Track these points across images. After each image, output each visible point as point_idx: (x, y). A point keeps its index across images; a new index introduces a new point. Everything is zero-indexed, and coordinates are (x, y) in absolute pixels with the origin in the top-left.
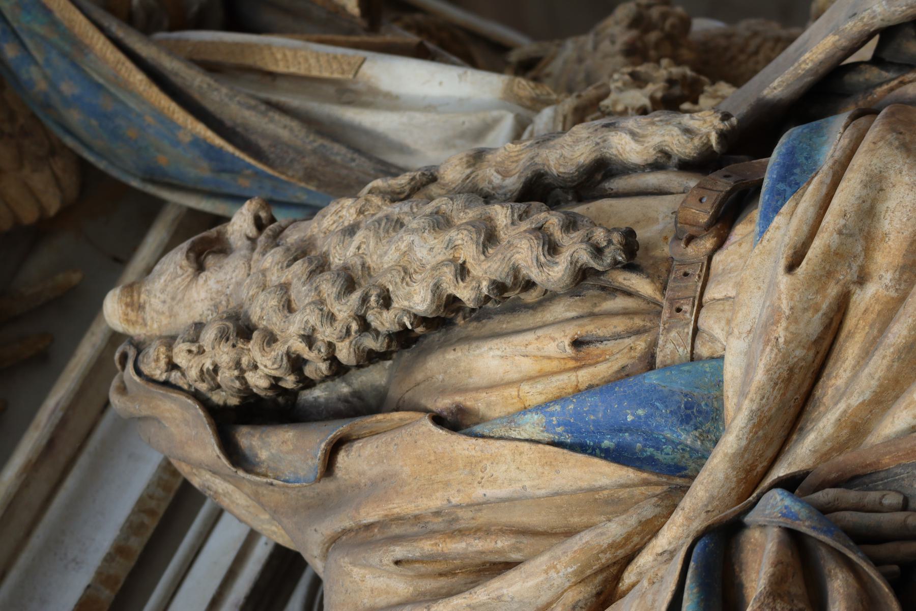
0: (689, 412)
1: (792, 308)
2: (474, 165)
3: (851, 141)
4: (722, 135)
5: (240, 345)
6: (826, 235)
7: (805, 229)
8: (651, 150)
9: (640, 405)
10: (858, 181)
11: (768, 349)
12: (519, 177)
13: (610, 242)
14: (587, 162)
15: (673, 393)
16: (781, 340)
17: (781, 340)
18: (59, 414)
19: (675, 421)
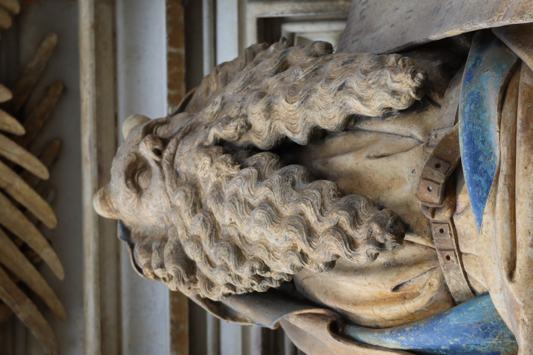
0: (486, 331)
1: (523, 302)
2: (270, 116)
3: (508, 149)
4: (417, 91)
5: (192, 287)
6: (523, 250)
7: (508, 242)
8: (377, 111)
9: (454, 336)
10: (527, 204)
11: (520, 327)
12: (303, 134)
13: (386, 240)
14: (340, 122)
15: (471, 325)
16: (526, 320)
17: (526, 320)
18: (95, 151)
19: (480, 339)
